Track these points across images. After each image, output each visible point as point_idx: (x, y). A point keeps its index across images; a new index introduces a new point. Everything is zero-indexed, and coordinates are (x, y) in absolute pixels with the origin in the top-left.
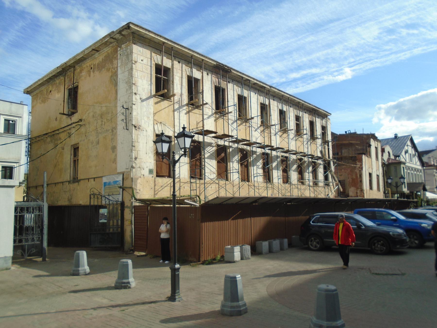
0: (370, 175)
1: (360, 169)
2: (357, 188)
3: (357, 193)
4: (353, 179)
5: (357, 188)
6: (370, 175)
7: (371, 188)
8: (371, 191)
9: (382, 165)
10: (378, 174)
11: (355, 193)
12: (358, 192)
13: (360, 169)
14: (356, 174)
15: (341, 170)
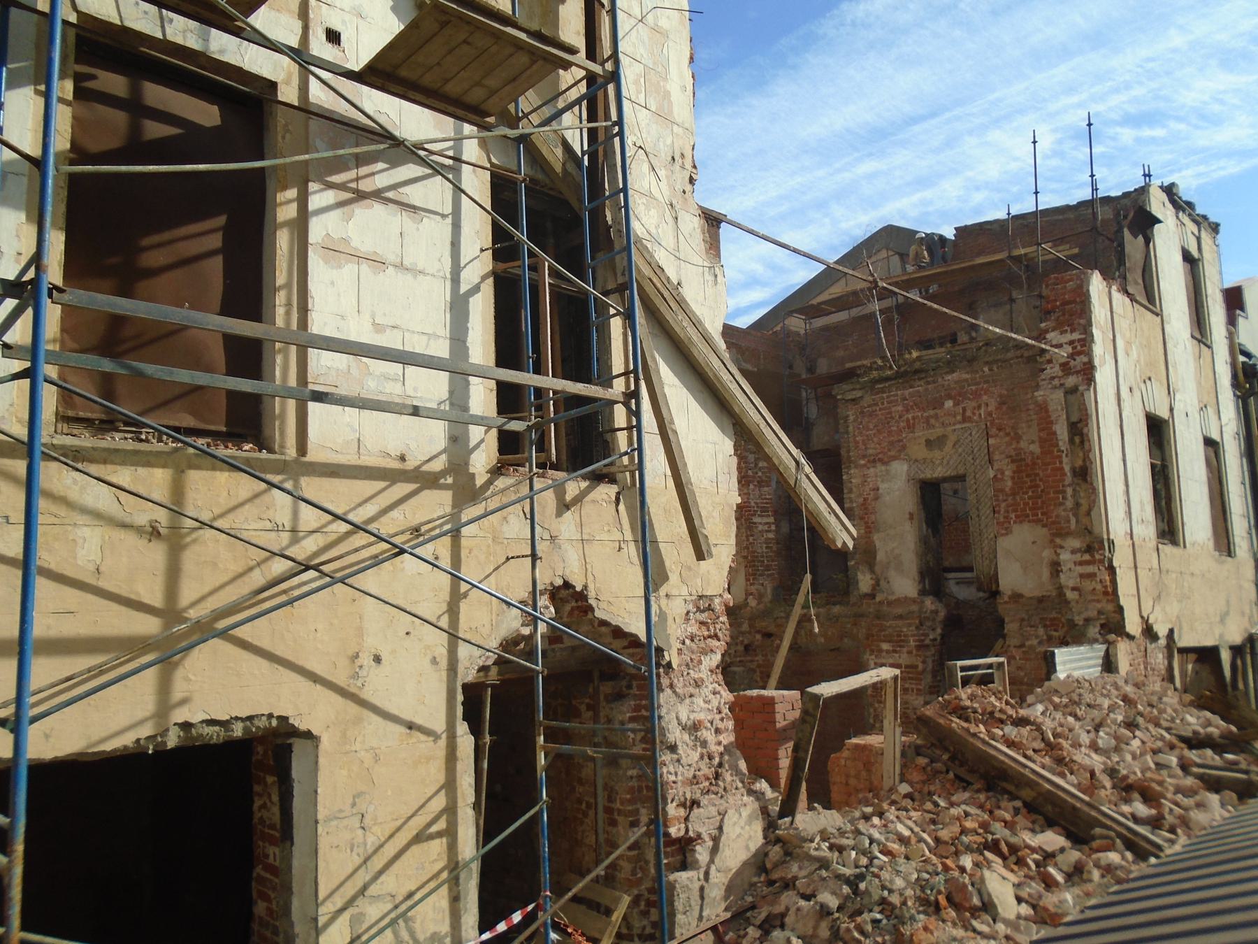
0: (1158, 430)
1: (1071, 381)
2: (1058, 533)
3: (1056, 568)
4: (1017, 459)
5: (1058, 533)
6: (1158, 430)
7: (1169, 530)
8: (1167, 549)
9: (1236, 384)
10: (1215, 436)
11: (1046, 573)
12: (1065, 556)
13: (1071, 381)
14: (1046, 424)
15: (938, 404)
